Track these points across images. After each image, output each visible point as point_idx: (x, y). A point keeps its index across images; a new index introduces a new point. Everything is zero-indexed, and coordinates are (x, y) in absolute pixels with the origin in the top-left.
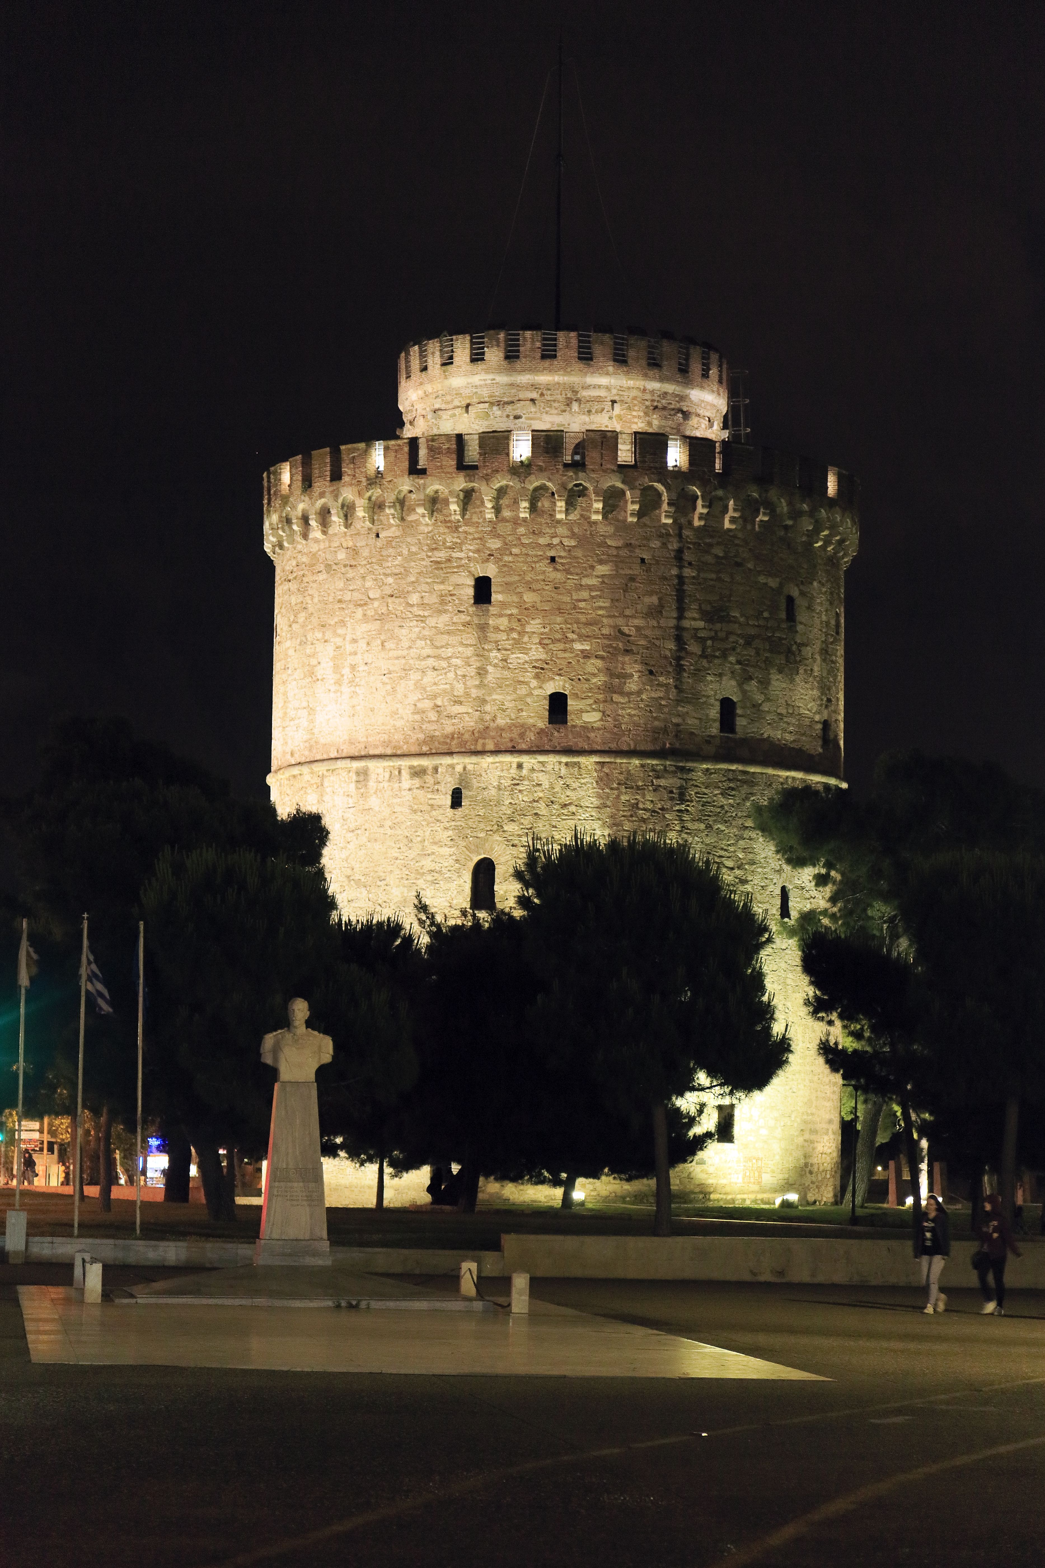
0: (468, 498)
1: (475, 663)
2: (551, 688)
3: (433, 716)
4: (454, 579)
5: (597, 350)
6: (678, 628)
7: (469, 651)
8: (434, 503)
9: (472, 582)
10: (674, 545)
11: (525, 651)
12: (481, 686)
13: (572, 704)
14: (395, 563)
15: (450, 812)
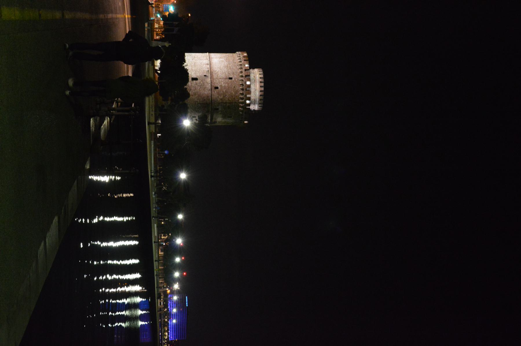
0: (242, 76)
1: (222, 78)
2: (219, 87)
3: (215, 73)
4: (232, 75)
5: (261, 92)
6: (227, 103)
7: (223, 77)
8: (241, 72)
9: (232, 77)
10: (237, 102)
11: (223, 84)
12: (219, 79)
13: (217, 90)
14: (234, 68)
15: (203, 75)
